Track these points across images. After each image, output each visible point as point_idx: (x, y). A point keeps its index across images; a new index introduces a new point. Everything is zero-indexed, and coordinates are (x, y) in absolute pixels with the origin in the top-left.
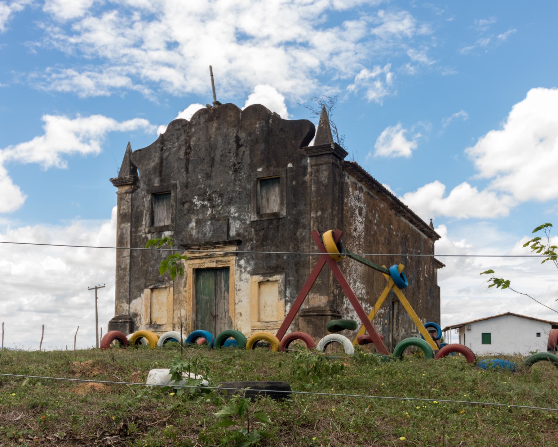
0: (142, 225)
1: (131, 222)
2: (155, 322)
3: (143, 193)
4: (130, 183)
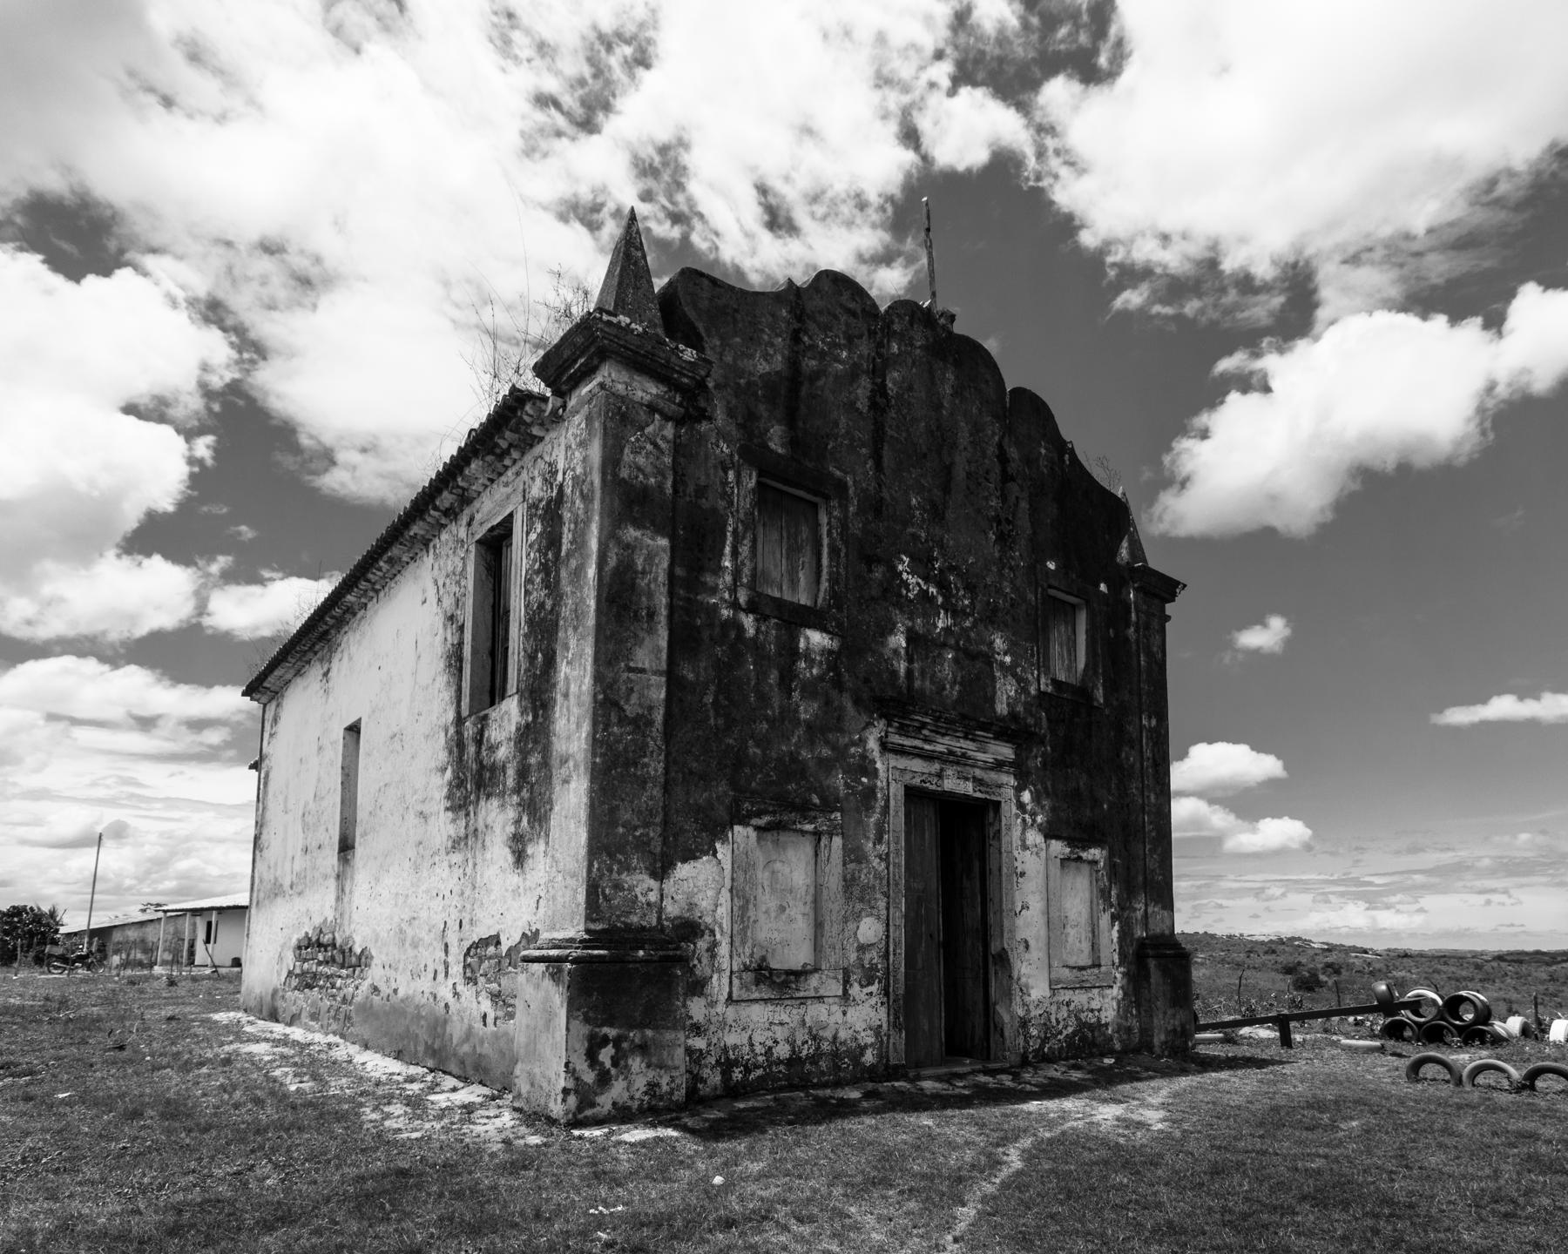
2: (763, 959)
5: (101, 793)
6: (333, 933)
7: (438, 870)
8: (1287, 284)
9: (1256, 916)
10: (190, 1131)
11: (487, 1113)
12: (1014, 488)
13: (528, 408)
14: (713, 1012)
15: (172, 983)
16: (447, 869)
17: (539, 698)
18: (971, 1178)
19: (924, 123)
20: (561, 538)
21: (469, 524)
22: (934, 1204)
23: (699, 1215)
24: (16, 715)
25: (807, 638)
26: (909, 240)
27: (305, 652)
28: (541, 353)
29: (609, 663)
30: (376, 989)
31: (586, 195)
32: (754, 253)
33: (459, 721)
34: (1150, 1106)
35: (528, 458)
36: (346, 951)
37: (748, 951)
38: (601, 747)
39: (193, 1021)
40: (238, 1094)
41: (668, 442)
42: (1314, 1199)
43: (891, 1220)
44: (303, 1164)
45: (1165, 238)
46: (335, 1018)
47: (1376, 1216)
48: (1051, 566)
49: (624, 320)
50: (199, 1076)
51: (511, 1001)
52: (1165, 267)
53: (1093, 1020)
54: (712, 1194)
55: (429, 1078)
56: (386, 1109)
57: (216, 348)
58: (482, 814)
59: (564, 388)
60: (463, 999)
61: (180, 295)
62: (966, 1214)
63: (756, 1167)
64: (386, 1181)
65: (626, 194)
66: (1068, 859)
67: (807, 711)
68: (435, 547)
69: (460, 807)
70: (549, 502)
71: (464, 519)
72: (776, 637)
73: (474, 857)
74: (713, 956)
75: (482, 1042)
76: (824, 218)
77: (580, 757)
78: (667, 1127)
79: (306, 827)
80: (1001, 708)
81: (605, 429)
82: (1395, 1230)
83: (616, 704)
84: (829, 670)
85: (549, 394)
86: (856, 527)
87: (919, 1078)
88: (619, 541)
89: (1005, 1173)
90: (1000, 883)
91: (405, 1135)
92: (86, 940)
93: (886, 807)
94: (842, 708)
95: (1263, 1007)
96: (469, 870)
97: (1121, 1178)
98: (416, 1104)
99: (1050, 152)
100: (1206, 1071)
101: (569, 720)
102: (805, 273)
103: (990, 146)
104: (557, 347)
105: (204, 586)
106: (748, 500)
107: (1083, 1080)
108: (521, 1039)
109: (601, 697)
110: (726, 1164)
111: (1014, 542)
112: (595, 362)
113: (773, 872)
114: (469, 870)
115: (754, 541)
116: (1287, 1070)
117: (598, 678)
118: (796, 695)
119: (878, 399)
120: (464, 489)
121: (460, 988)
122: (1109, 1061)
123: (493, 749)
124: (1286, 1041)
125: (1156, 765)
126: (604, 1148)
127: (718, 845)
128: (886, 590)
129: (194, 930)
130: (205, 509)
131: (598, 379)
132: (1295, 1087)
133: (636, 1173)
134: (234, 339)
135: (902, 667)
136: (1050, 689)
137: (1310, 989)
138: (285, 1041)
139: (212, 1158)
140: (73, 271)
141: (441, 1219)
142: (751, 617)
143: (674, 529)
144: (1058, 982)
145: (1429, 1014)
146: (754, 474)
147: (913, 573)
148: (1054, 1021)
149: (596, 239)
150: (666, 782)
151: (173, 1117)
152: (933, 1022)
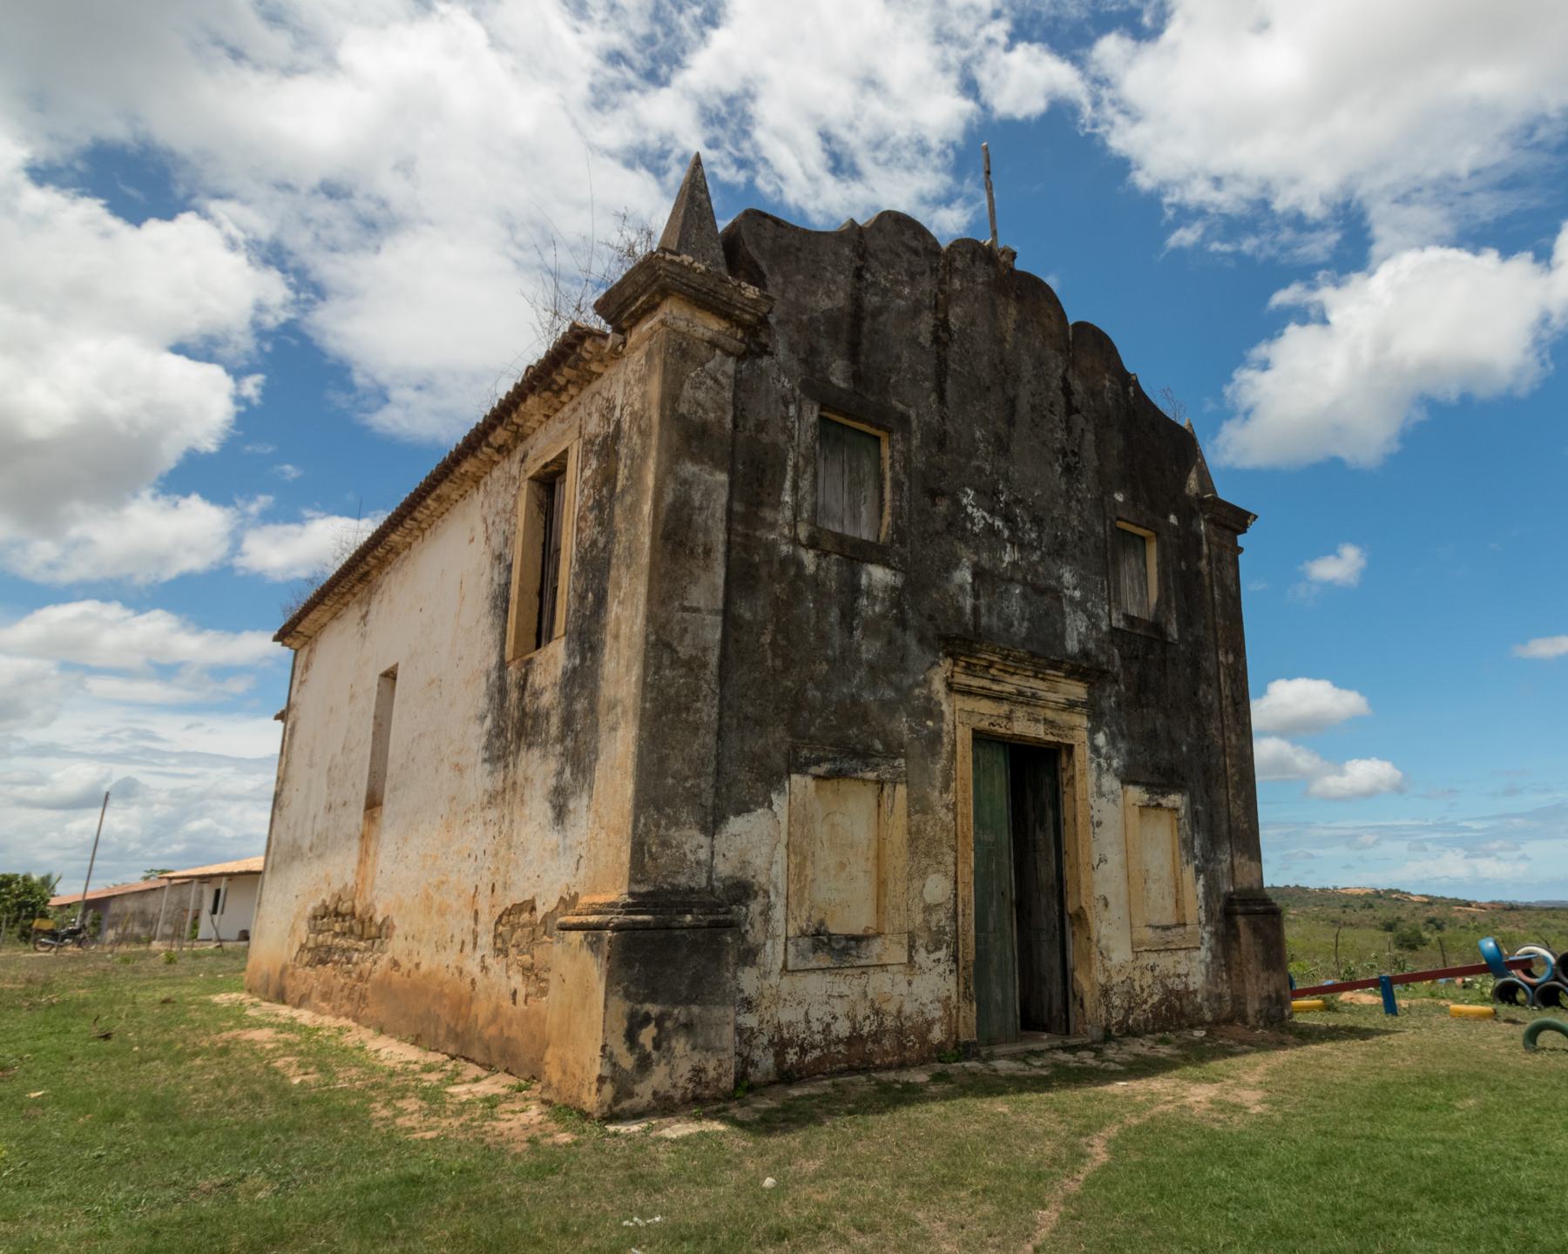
0: (777, 505)
1: (732, 473)
3: (788, 385)
4: (747, 317)
5: (111, 747)
6: (353, 900)
7: (472, 829)
8: (1341, 222)
9: (1348, 867)
10: (176, 1134)
11: (512, 1107)
12: (1078, 420)
13: (588, 344)
14: (766, 984)
15: (170, 961)
16: (481, 828)
17: (587, 641)
18: (1052, 1174)
19: (983, 76)
20: (616, 473)
21: (522, 461)
22: (1011, 1206)
23: (747, 1225)
24: (28, 664)
25: (869, 574)
26: (967, 181)
27: (344, 594)
28: (603, 291)
29: (663, 603)
30: (396, 964)
31: (652, 140)
32: (817, 195)
33: (502, 665)
34: (1246, 1086)
35: (586, 393)
36: (366, 921)
37: (805, 915)
38: (652, 692)
39: (190, 1004)
40: (234, 1088)
41: (729, 377)
42: (1433, 1192)
43: (963, 1227)
44: (301, 1172)
45: (1217, 182)
46: (349, 998)
47: (1504, 1212)
48: (1119, 497)
49: (687, 259)
50: (191, 1069)
51: (545, 975)
52: (1219, 207)
53: (1181, 987)
54: (763, 1200)
55: (449, 1067)
56: (399, 1105)
57: (274, 288)
58: (522, 764)
59: (625, 325)
60: (491, 974)
61: (240, 236)
62: (1048, 1217)
63: (811, 1166)
64: (394, 1191)
65: (693, 142)
66: (1148, 806)
67: (870, 650)
68: (485, 484)
69: (499, 758)
70: (605, 439)
71: (518, 456)
72: (837, 574)
73: (512, 813)
74: (767, 921)
75: (510, 1024)
76: (887, 163)
77: (629, 702)
78: (712, 1119)
79: (331, 782)
80: (1072, 645)
81: (665, 364)
82: (1526, 1229)
83: (668, 646)
84: (892, 607)
85: (609, 331)
86: (919, 461)
87: (991, 1057)
88: (676, 477)
89: (1088, 1168)
90: (1076, 835)
91: (419, 1135)
92: (80, 912)
93: (954, 752)
94: (905, 647)
95: (1364, 969)
96: (505, 828)
97: (1219, 1172)
98: (433, 1099)
99: (1106, 102)
100: (1306, 1044)
101: (618, 664)
102: (866, 213)
103: (1047, 95)
104: (620, 285)
105: (242, 527)
106: (809, 434)
107: (1172, 1056)
108: (553, 1019)
109: (653, 638)
110: (778, 1163)
111: (1081, 474)
112: (657, 299)
113: (833, 825)
114: (505, 828)
115: (815, 475)
116: (1394, 1040)
117: (650, 618)
118: (858, 634)
119: (940, 333)
120: (519, 426)
121: (489, 961)
122: (1199, 1034)
123: (536, 694)
124: (1390, 1007)
125: (1235, 703)
126: (642, 1147)
127: (774, 796)
128: (950, 525)
129: (200, 900)
130: (249, 448)
131: (660, 315)
132: (1403, 1060)
133: (678, 1176)
134: (292, 280)
135: (968, 603)
136: (1122, 625)
137: (1413, 948)
138: (291, 1026)
139: (198, 1167)
140: (135, 216)
141: (454, 1237)
142: (811, 553)
143: (733, 465)
144: (1141, 943)
145: (1542, 976)
146: (816, 408)
147: (978, 506)
148: (1137, 988)
149: (662, 184)
150: (720, 728)
151: (158, 1118)
152: (1007, 993)
